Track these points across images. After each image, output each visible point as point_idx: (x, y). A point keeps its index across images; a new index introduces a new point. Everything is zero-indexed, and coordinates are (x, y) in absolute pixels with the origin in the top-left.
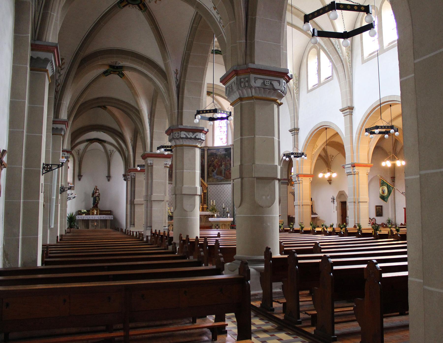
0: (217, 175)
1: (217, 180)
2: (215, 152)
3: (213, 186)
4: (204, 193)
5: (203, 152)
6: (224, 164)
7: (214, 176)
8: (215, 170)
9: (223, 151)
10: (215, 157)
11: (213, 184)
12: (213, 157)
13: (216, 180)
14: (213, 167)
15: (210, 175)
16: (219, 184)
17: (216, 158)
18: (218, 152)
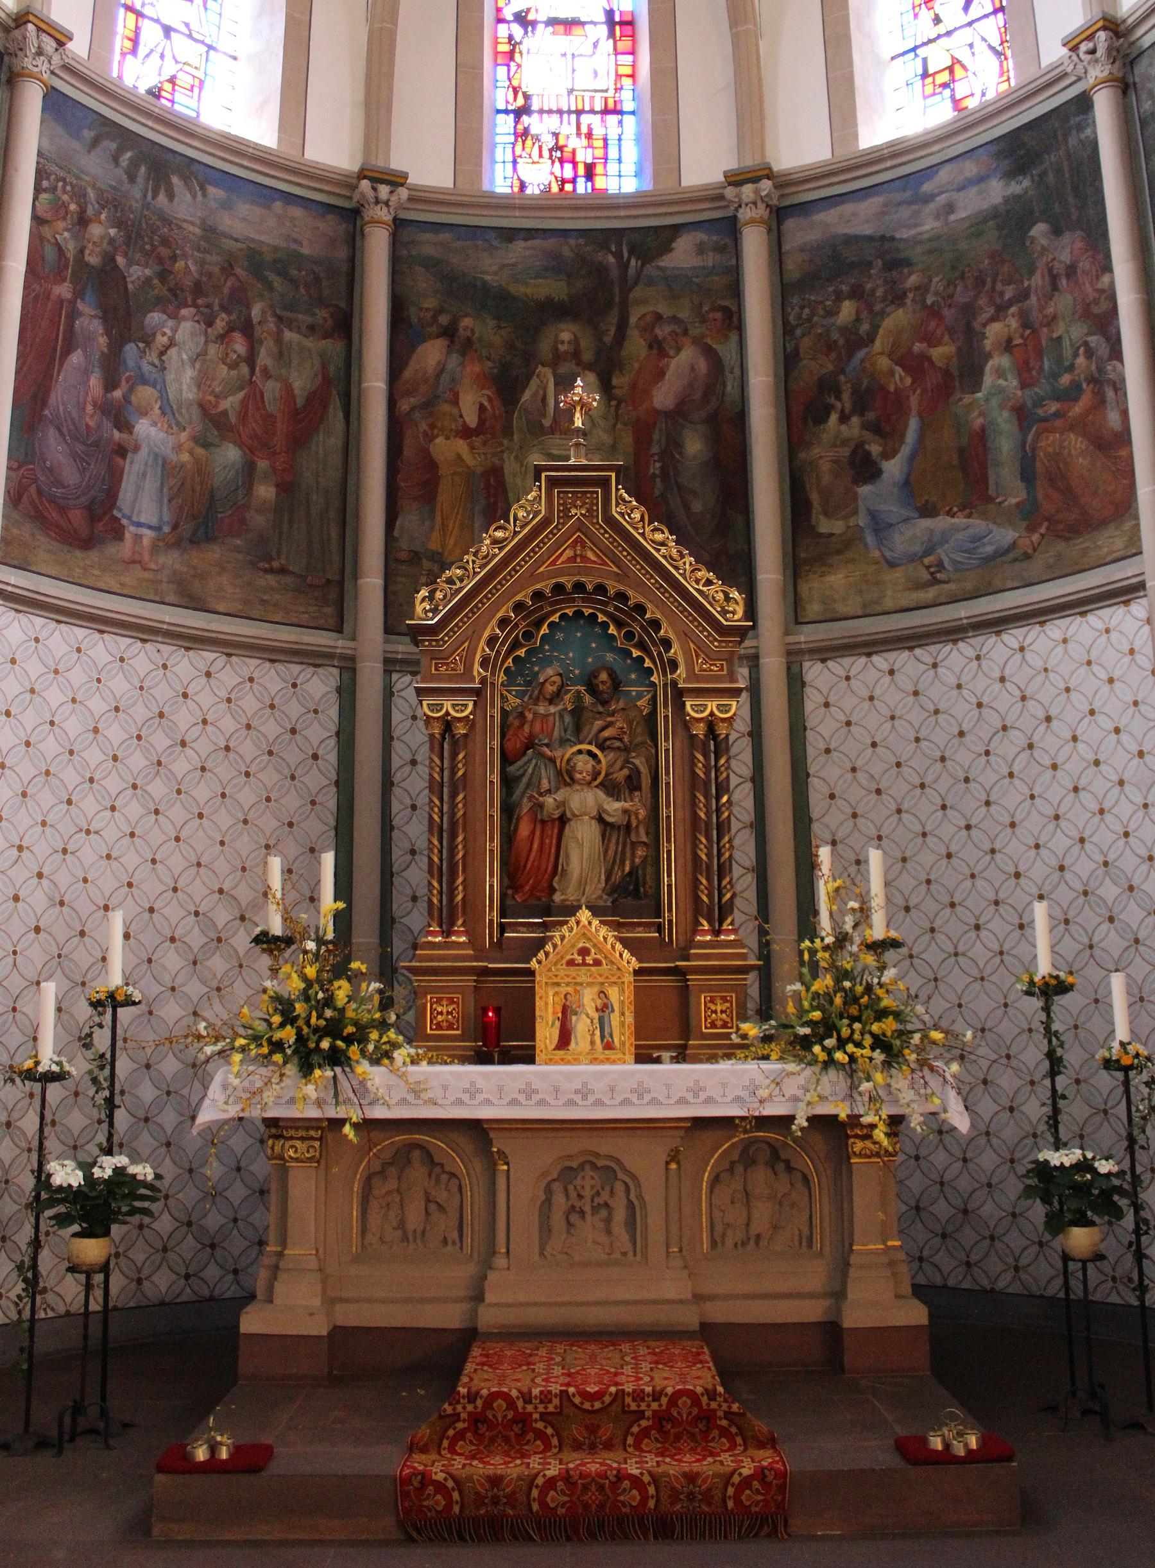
0: (928, 511)
1: (935, 581)
2: (868, 230)
3: (871, 675)
4: (699, 730)
5: (720, 249)
6: (1008, 346)
7: (881, 527)
8: (888, 455)
9: (981, 179)
10: (875, 284)
11: (868, 647)
12: (857, 293)
13: (920, 586)
14: (855, 420)
15: (825, 526)
16: (953, 633)
17: (898, 299)
18: (905, 213)
